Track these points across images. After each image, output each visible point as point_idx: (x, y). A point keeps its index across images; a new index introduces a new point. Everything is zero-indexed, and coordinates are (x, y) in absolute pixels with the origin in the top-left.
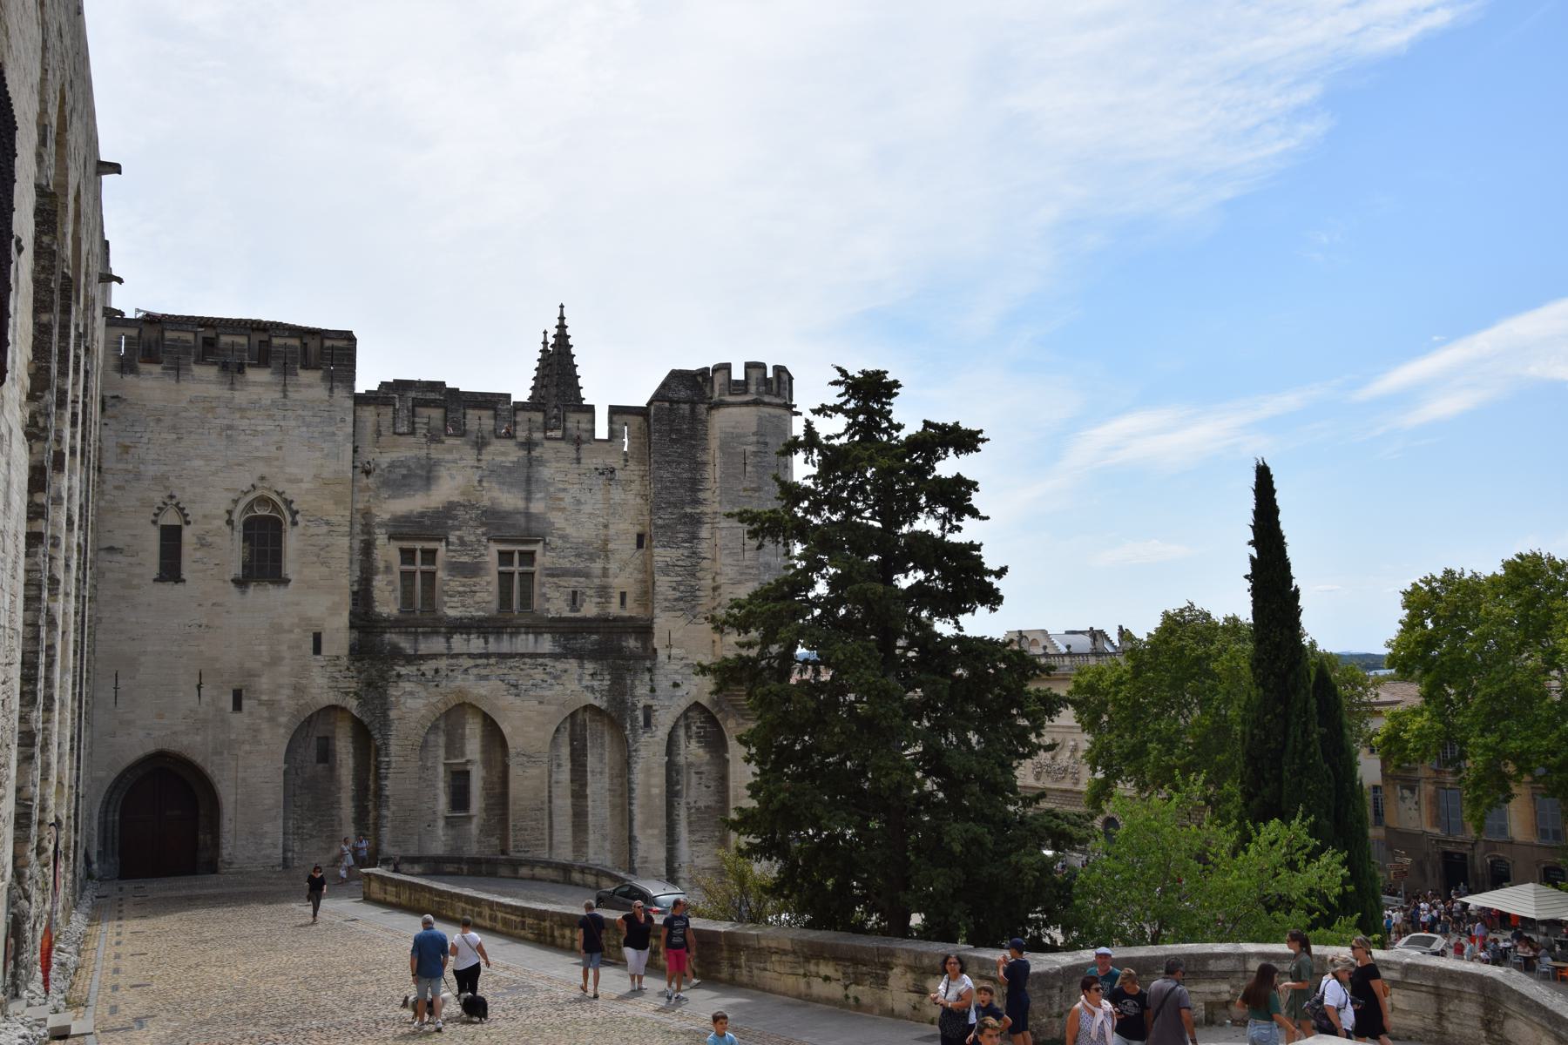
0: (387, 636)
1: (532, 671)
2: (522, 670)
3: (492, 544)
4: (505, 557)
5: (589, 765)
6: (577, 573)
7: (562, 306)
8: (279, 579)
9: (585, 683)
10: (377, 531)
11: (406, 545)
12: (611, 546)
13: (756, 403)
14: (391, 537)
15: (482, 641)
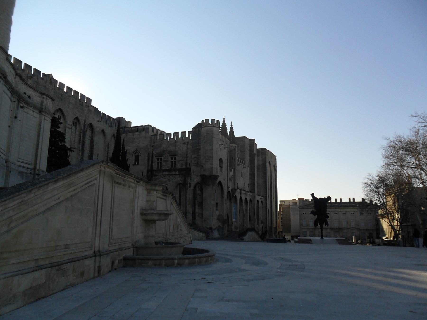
0: (154, 173)
1: (172, 177)
2: (170, 177)
3: (170, 157)
4: (172, 159)
5: (182, 194)
6: (182, 160)
7: (224, 116)
8: (138, 164)
9: (180, 179)
10: (154, 156)
11: (157, 158)
12: (188, 155)
13: (206, 126)
14: (156, 157)
15: (168, 173)
